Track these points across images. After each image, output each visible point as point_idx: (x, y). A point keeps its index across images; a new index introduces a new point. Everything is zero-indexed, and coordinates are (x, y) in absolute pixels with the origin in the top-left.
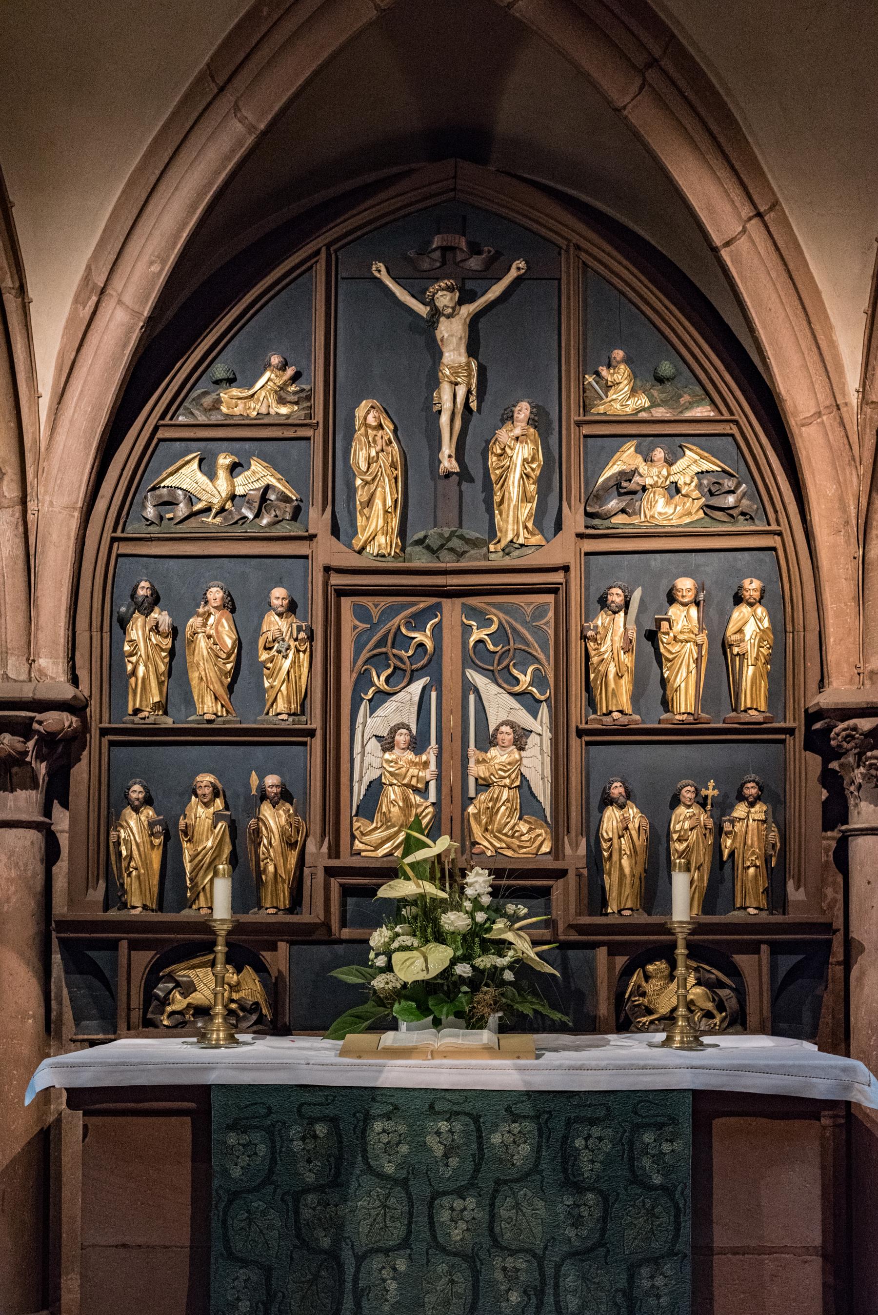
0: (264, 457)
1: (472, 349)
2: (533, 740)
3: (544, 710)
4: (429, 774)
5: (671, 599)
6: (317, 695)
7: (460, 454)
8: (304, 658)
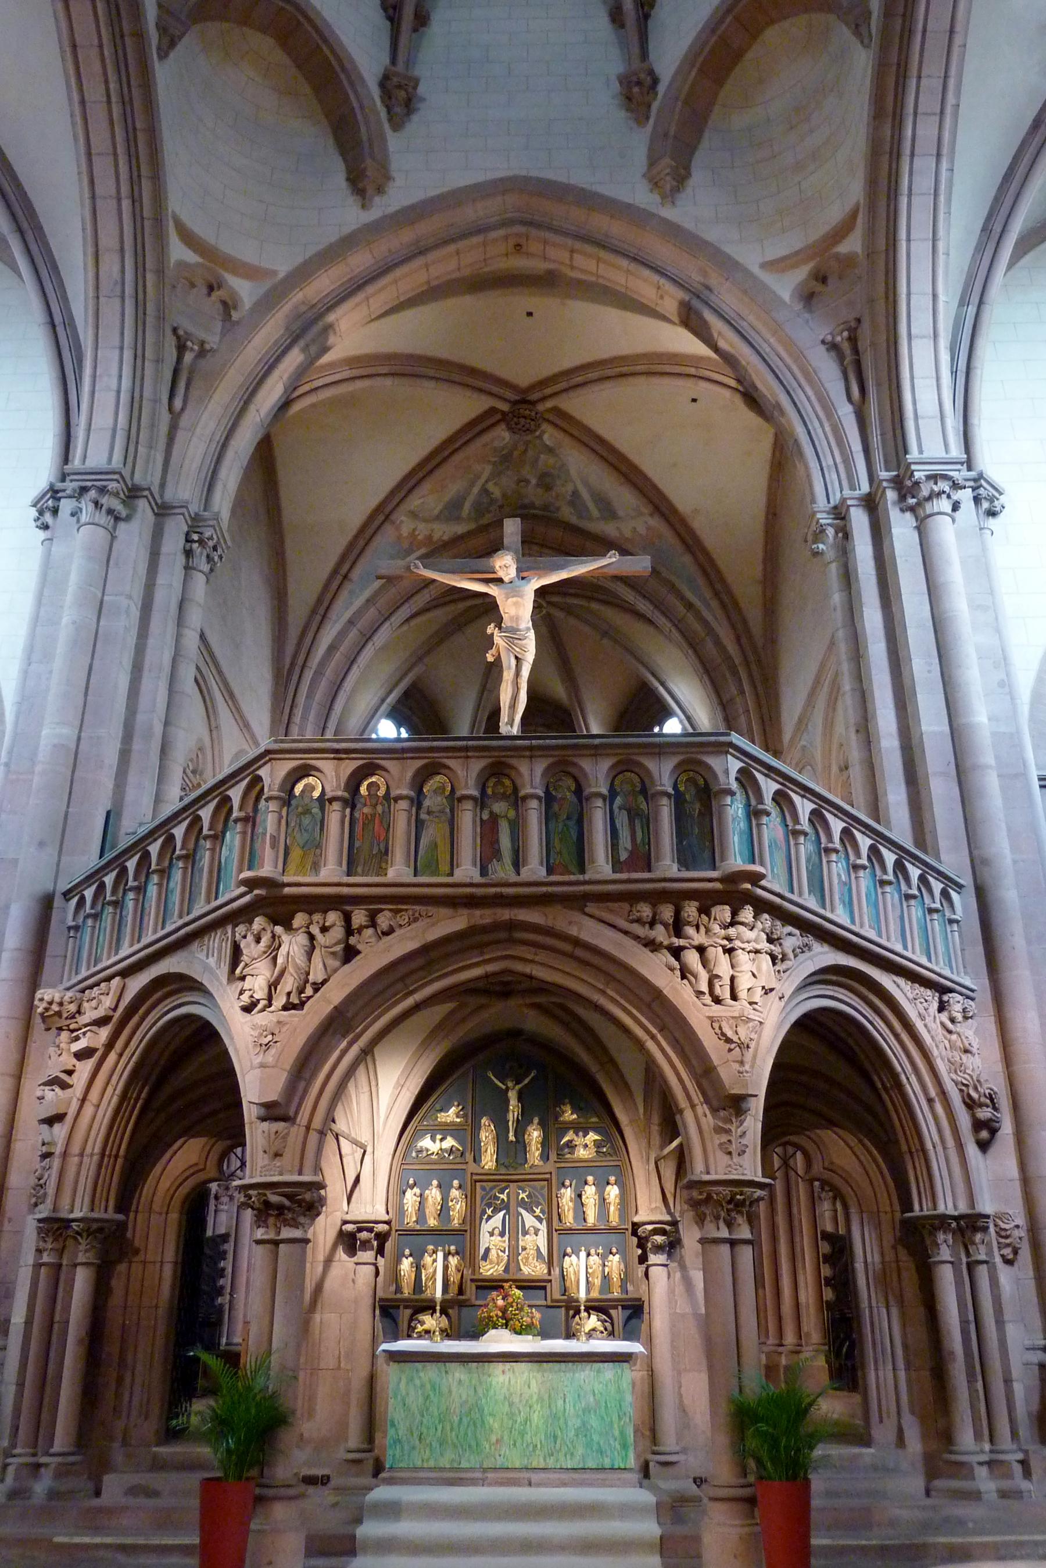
0: (451, 1136)
1: (520, 1099)
2: (540, 1232)
3: (544, 1222)
4: (506, 1245)
5: (586, 1183)
6: (468, 1218)
7: (516, 1135)
8: (464, 1204)
